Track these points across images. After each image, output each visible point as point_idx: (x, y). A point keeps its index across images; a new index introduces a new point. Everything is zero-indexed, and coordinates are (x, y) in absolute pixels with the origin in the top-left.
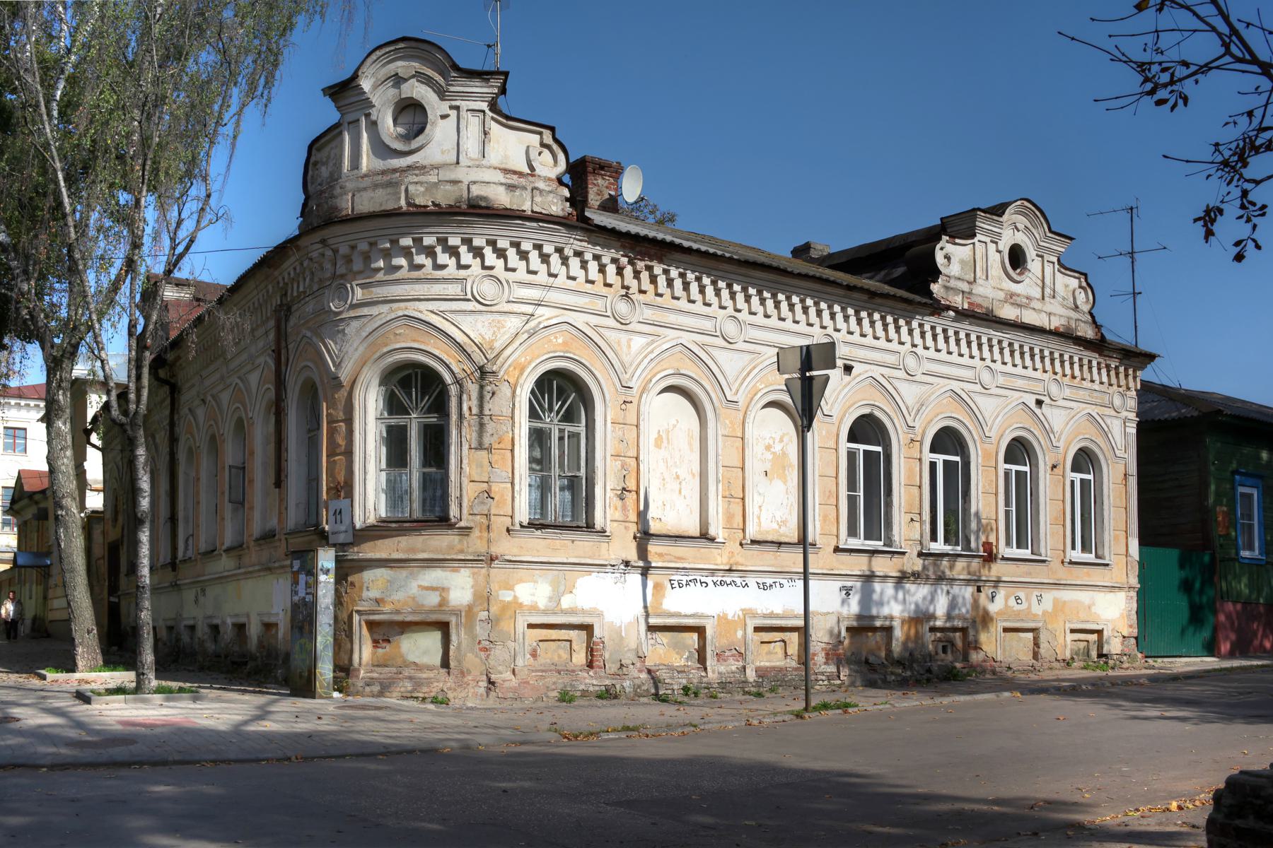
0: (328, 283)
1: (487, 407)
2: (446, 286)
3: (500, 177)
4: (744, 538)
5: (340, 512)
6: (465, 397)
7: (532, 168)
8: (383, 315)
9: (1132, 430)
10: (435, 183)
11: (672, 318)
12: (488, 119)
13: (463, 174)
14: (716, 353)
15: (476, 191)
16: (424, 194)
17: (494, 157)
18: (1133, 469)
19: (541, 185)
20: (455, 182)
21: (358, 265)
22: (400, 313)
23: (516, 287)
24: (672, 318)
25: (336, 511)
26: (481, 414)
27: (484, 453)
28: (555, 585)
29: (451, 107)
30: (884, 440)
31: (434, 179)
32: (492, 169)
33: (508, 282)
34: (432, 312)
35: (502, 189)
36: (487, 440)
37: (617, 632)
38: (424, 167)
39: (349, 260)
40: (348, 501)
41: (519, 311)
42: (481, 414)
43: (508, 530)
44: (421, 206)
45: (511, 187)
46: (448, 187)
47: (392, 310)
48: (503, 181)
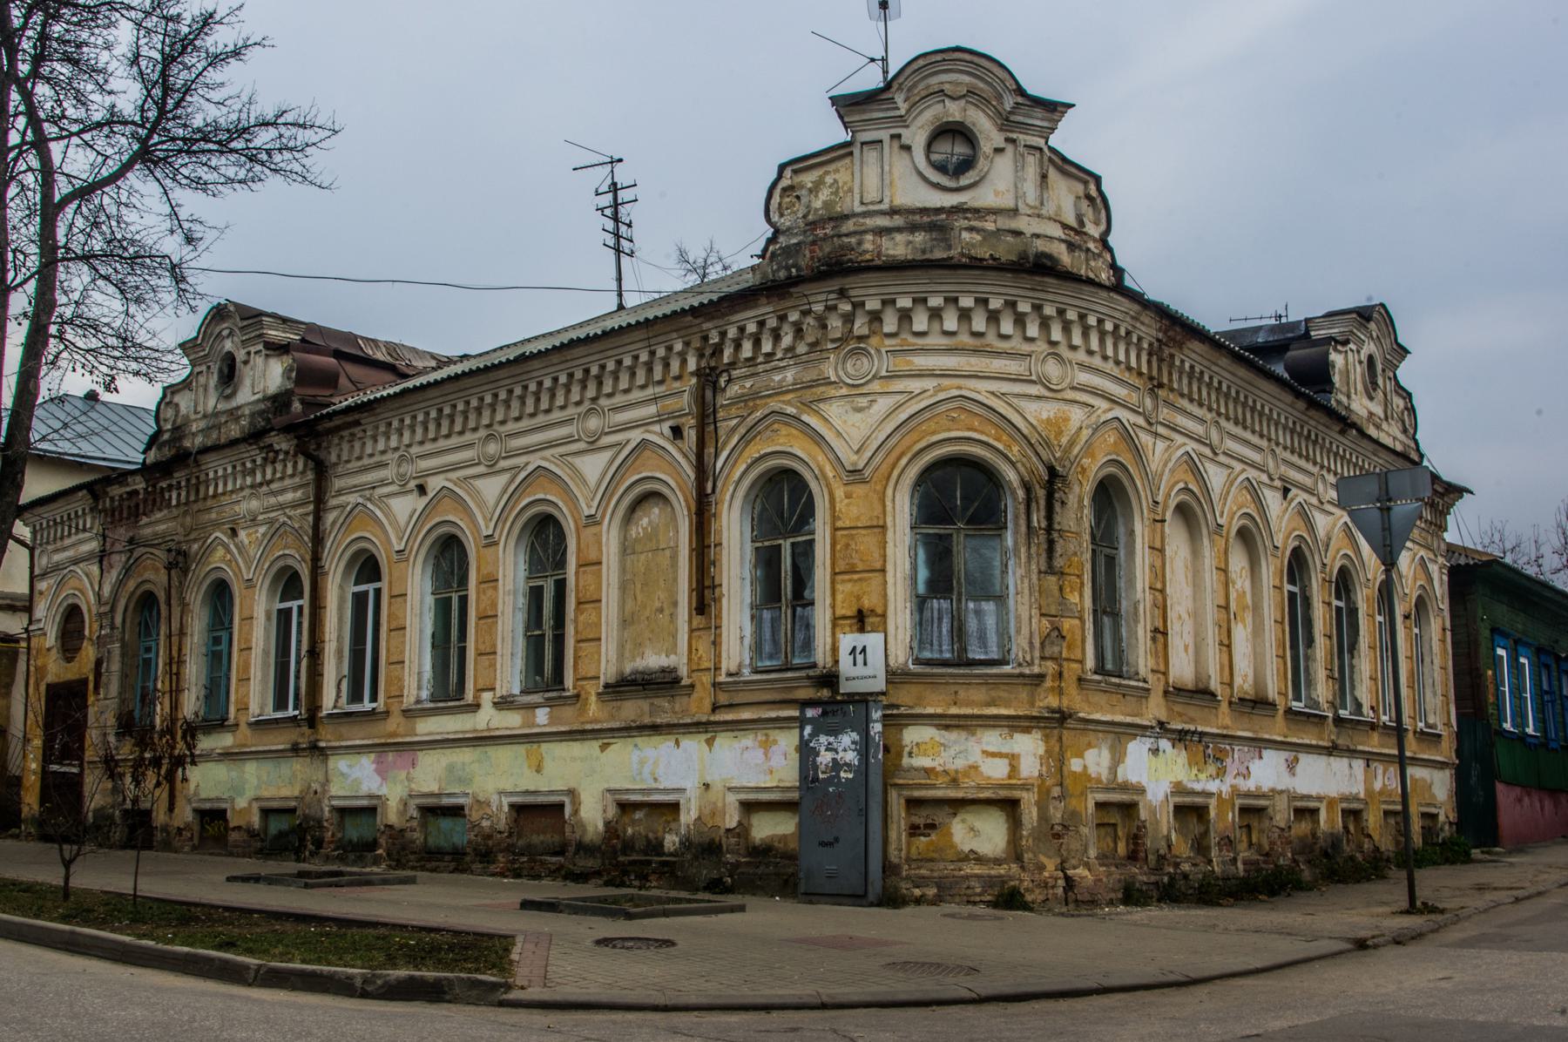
0: (830, 346)
1: (1057, 518)
2: (1008, 362)
3: (1057, 232)
4: (1232, 696)
5: (864, 650)
6: (1034, 505)
7: (1082, 224)
8: (928, 393)
9: (1445, 578)
10: (993, 232)
11: (1181, 420)
12: (1046, 158)
13: (1024, 224)
14: (1207, 465)
15: (1041, 246)
16: (981, 244)
17: (1049, 209)
18: (1448, 625)
19: (1091, 245)
20: (1017, 233)
21: (890, 323)
22: (956, 392)
23: (1076, 371)
24: (1181, 420)
25: (854, 648)
26: (1049, 529)
27: (1053, 579)
28: (1112, 749)
29: (1007, 140)
30: (1301, 579)
31: (990, 226)
32: (1052, 222)
33: (1070, 362)
34: (993, 393)
35: (1063, 247)
36: (1058, 563)
37: (1153, 812)
38: (976, 211)
39: (876, 317)
40: (879, 637)
41: (1081, 400)
42: (1049, 529)
43: (1080, 680)
44: (976, 259)
45: (1071, 246)
46: (1009, 239)
47: (939, 389)
48: (1063, 237)
